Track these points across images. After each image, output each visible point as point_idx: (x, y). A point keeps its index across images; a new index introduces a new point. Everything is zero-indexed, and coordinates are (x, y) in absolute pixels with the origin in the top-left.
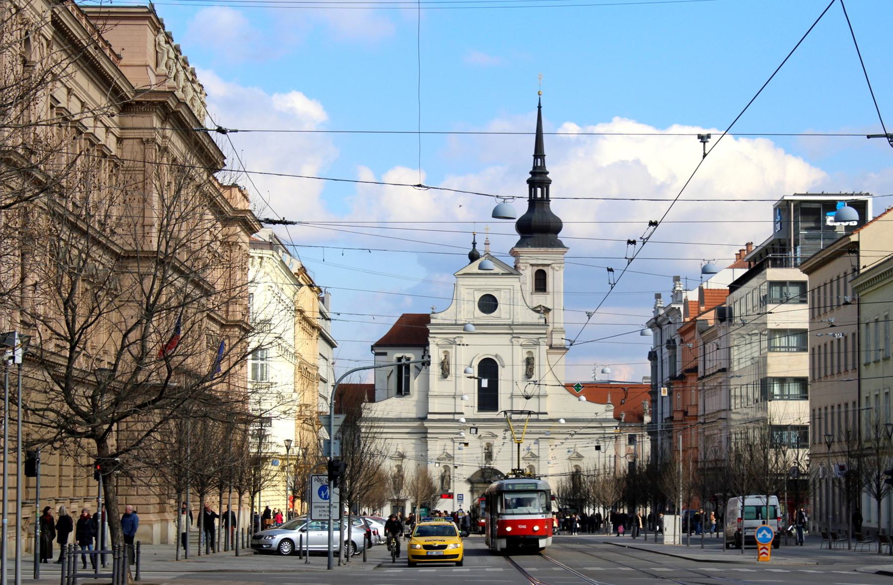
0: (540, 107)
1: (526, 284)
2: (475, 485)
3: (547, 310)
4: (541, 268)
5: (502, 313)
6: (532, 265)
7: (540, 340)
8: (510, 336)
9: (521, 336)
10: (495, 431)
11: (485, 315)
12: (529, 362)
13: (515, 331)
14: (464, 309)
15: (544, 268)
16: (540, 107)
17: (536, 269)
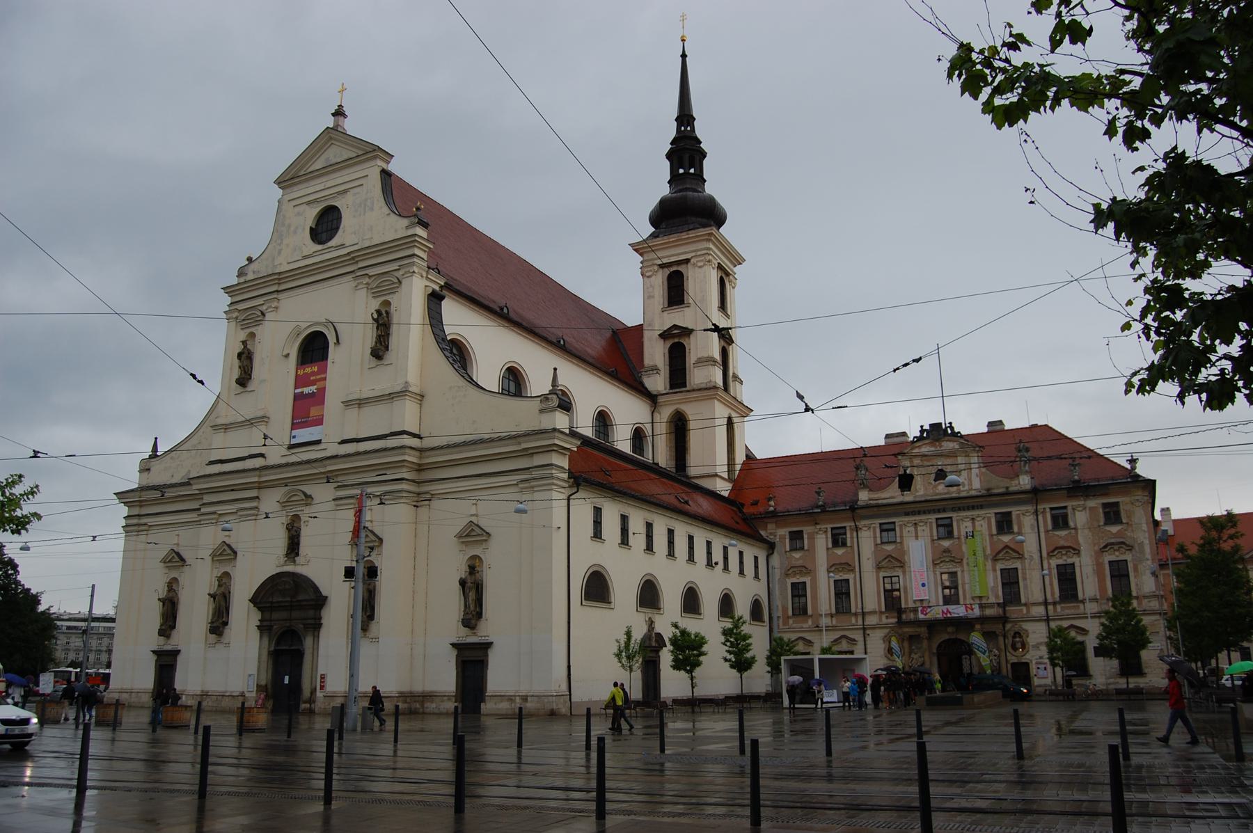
0: (684, 56)
1: (653, 297)
2: (276, 615)
3: (687, 332)
4: (675, 268)
5: (349, 235)
6: (662, 266)
7: (401, 272)
8: (349, 277)
9: (371, 272)
10: (308, 489)
11: (320, 247)
12: (383, 323)
13: (361, 265)
14: (288, 245)
15: (681, 268)
16: (684, 56)
17: (667, 271)
